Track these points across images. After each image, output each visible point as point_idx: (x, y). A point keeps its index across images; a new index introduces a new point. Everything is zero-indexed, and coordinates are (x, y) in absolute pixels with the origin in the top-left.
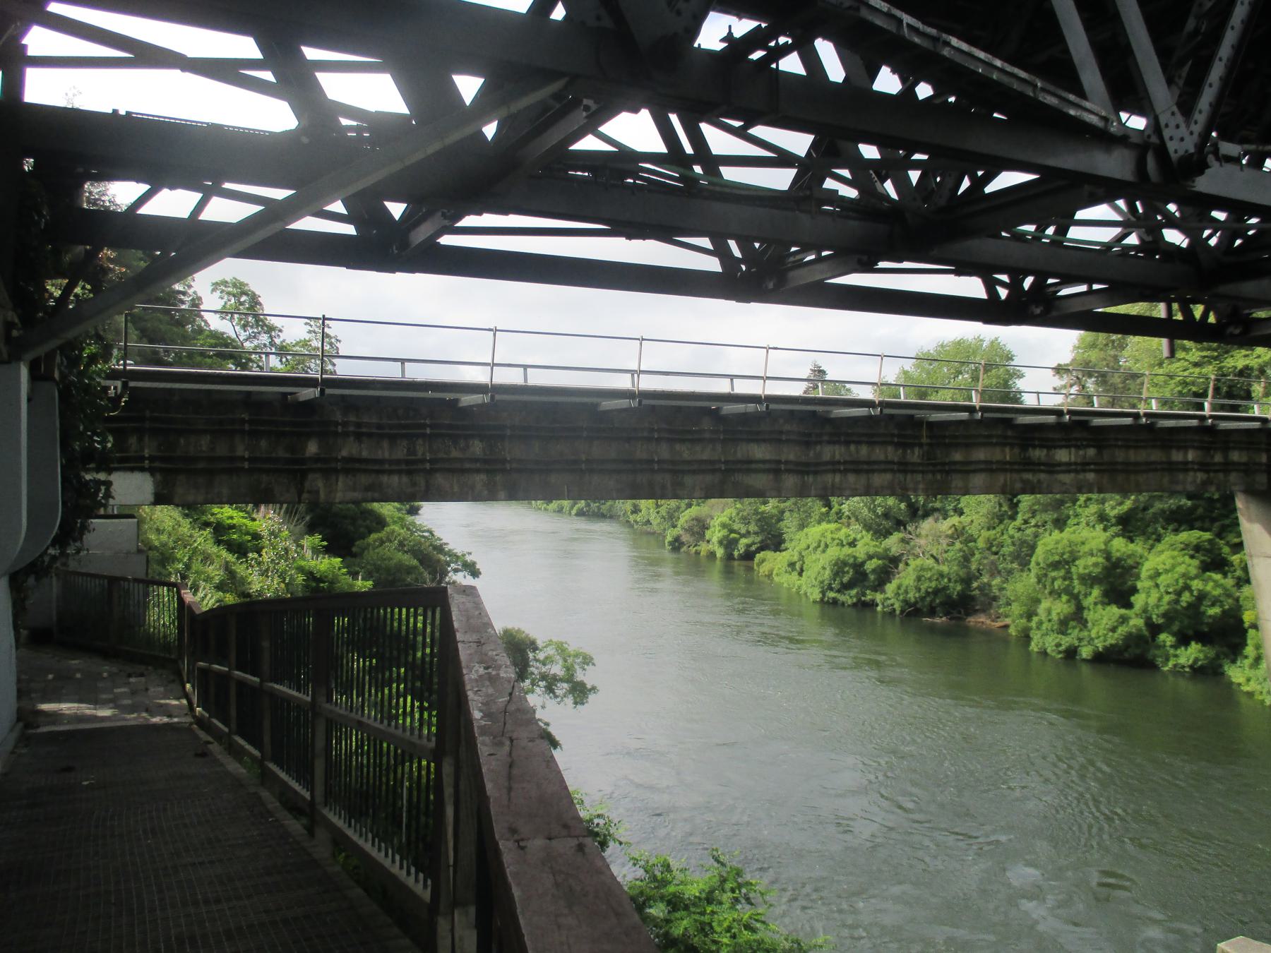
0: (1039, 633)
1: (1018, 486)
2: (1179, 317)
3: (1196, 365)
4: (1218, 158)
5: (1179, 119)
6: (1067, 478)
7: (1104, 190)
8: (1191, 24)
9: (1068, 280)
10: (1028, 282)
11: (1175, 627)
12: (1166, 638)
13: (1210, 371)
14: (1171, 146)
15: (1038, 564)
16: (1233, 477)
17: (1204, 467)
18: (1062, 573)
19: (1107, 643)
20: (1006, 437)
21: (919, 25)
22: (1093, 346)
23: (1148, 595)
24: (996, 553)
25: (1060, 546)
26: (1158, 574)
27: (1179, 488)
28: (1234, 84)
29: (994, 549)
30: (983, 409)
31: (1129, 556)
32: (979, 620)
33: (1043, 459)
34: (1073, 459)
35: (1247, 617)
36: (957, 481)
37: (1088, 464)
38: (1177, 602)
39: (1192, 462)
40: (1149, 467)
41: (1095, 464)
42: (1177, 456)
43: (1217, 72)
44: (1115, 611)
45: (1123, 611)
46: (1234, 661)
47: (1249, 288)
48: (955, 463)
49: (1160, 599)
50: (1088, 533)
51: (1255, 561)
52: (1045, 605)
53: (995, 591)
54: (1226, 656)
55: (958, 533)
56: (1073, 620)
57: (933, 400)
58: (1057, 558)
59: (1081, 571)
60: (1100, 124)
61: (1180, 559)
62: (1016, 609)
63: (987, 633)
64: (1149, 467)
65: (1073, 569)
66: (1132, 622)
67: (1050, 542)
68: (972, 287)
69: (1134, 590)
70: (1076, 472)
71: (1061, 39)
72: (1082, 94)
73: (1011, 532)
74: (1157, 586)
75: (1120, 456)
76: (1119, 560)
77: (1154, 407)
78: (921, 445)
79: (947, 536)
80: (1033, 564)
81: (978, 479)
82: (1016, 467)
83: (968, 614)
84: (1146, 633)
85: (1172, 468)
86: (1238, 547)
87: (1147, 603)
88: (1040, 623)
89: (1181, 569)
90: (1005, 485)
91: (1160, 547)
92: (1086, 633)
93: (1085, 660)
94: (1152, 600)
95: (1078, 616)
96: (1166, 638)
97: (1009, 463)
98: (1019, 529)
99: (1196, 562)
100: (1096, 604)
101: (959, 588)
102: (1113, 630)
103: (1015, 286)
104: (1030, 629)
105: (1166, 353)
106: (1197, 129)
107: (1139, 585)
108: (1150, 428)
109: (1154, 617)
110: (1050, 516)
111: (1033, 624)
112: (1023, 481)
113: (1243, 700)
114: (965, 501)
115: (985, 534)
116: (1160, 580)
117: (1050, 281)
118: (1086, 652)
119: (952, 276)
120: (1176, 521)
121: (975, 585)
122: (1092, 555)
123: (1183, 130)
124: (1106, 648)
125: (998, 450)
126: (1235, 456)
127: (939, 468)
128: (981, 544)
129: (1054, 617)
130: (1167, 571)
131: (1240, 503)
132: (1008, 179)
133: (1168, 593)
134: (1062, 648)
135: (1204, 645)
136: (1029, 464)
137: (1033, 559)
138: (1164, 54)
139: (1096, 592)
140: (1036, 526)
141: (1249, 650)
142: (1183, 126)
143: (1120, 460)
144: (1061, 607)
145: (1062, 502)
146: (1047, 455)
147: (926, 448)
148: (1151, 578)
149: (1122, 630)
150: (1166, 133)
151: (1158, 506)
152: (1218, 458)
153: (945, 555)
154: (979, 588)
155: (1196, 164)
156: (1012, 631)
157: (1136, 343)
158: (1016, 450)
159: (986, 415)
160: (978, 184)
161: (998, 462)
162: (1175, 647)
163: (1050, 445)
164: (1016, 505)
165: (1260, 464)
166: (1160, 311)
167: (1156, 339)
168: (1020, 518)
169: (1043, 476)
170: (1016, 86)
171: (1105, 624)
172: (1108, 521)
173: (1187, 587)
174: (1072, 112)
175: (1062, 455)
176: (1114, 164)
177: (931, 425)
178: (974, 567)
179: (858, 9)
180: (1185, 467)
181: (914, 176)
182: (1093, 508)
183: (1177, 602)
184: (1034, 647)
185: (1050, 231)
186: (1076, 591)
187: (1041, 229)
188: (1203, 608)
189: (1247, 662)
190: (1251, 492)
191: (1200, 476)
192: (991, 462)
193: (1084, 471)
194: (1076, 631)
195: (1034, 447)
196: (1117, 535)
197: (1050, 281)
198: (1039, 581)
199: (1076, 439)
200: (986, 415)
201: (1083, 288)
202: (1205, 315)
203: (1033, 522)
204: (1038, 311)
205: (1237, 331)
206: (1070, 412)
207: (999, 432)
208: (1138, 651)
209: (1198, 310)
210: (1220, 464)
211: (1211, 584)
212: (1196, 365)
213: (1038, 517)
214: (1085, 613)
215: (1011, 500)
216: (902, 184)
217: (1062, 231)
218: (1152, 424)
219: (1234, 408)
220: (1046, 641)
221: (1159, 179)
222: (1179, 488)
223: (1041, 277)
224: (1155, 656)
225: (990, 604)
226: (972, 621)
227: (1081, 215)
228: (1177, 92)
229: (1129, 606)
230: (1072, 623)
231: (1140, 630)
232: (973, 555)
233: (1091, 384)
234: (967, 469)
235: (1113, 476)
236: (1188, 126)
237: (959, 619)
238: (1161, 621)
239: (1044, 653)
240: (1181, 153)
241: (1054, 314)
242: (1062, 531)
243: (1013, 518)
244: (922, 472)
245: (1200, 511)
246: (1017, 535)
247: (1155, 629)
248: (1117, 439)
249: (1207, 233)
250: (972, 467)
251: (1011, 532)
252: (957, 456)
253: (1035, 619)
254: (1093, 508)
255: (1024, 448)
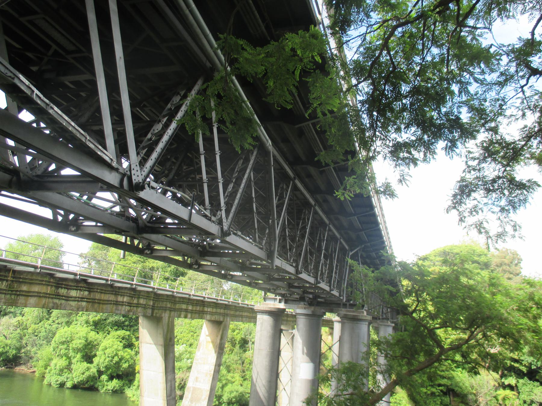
0: (49, 375)
1: (51, 305)
2: (129, 243)
3: (134, 263)
4: (149, 186)
5: (138, 168)
6: (73, 304)
7: (109, 187)
8: (149, 136)
9: (87, 219)
10: (71, 216)
11: (109, 373)
12: (104, 377)
13: (139, 266)
14: (134, 177)
15: (55, 342)
16: (140, 309)
17: (130, 304)
18: (65, 346)
19: (79, 380)
20: (50, 282)
21: (42, 96)
22: (97, 248)
23: (100, 358)
24: (36, 336)
25: (66, 334)
26: (106, 349)
27: (119, 312)
28: (160, 161)
29: (36, 334)
30: (41, 268)
31: (96, 340)
32: (21, 369)
33: (65, 294)
34: (78, 295)
35: (137, 368)
36: (22, 300)
37: (84, 298)
38: (111, 361)
39: (126, 302)
40: (108, 302)
41: (87, 299)
42: (120, 299)
43: (154, 156)
44: (85, 365)
45: (89, 365)
46: (129, 387)
47: (154, 237)
48: (23, 291)
49: (105, 359)
50: (79, 328)
51: (143, 344)
52: (54, 362)
53: (32, 354)
54: (127, 385)
55: (20, 325)
56: (66, 368)
57: (22, 260)
58: (64, 339)
59: (74, 346)
60: (109, 161)
61: (116, 343)
62: (41, 363)
63: (24, 376)
64: (108, 302)
65: (71, 345)
66: (91, 370)
67: (63, 332)
68: (46, 213)
69: (95, 355)
70: (78, 301)
71: (101, 124)
72: (105, 147)
73: (46, 326)
74: (105, 354)
75: (98, 296)
76: (91, 341)
77: (115, 277)
78: (7, 281)
79: (14, 326)
80: (53, 342)
81: (32, 300)
82: (52, 296)
83: (16, 366)
84: (96, 375)
85: (117, 303)
86: (137, 338)
87: (99, 362)
88: (51, 370)
89: (115, 347)
90: (45, 304)
91: (109, 336)
92: (71, 375)
93: (68, 388)
94: (102, 360)
95: (69, 368)
96: (104, 377)
97: (49, 294)
98: (50, 325)
99: (122, 344)
100: (77, 361)
101: (14, 352)
102: (83, 374)
103: (65, 217)
104: (45, 373)
105: (122, 256)
106: (144, 174)
107: (97, 353)
108: (112, 286)
109: (101, 368)
110: (65, 320)
111: (47, 371)
112: (54, 303)
113: (131, 403)
114: (26, 310)
115: (33, 326)
116: (106, 351)
117: (81, 218)
118: (69, 384)
119: (37, 206)
120: (117, 325)
121: (23, 351)
122: (80, 339)
123: (139, 173)
124: (78, 382)
125: (45, 287)
126: (142, 301)
127: (14, 292)
128: (30, 331)
129: (58, 367)
130: (110, 347)
131: (141, 320)
132: (67, 172)
133: (109, 357)
134: (59, 382)
135: (119, 380)
136: (58, 295)
137: (54, 339)
138: (138, 143)
139: (79, 356)
140: (58, 324)
141: (136, 383)
142: (139, 171)
143: (97, 298)
144: (63, 362)
145: (71, 314)
146: (67, 292)
147: (9, 282)
148: (103, 350)
149: (87, 374)
150: (133, 172)
151: (111, 319)
152: (135, 301)
153: (10, 335)
154: (24, 353)
155: (140, 187)
156: (37, 374)
157: (113, 250)
158: (53, 288)
159: (42, 271)
160: (58, 169)
161: (44, 293)
162: (107, 381)
163: (68, 288)
164: (51, 313)
165: (150, 305)
166: (122, 239)
167: (119, 250)
168: (51, 319)
169: (63, 302)
170: (78, 135)
171: (80, 371)
172: (89, 323)
173: (117, 355)
174: (99, 153)
175: (73, 293)
176: (112, 178)
177: (14, 272)
178: (24, 342)
179: (13, 79)
180: (122, 304)
181: (29, 158)
182: (84, 318)
183: (111, 361)
184: (45, 382)
185: (85, 197)
186: (70, 355)
187: (81, 196)
188: (121, 364)
189: (134, 388)
190: (145, 316)
191: (128, 308)
192: (40, 293)
193: (82, 301)
194: (67, 374)
195: (62, 288)
196: (92, 330)
197: (81, 218)
198: (54, 350)
199: (81, 287)
200: (42, 271)
201: (94, 224)
202: (139, 244)
203: (57, 321)
204: (73, 229)
205: (148, 252)
206: (80, 275)
207: (47, 279)
208: (92, 383)
209: (136, 242)
210: (135, 304)
211: (126, 353)
212: (134, 263)
213: (59, 320)
214: (72, 365)
215: (49, 311)
216: (22, 160)
217: (90, 199)
218: (113, 284)
219: (146, 282)
220: (52, 379)
221: (129, 189)
222: (119, 312)
223: (77, 215)
224: (98, 385)
225: (28, 361)
226: (17, 369)
227: (99, 194)
228: (140, 158)
229: (91, 362)
230: (66, 370)
231: (94, 374)
232: (25, 336)
233: (93, 263)
234: (28, 295)
235: (94, 304)
236: (141, 172)
237: (12, 368)
238: (103, 369)
239: (50, 385)
240: (137, 181)
241: (80, 232)
242: (69, 327)
243: (48, 319)
244: (5, 294)
245: (127, 323)
246: (48, 327)
247: (100, 373)
248: (98, 289)
249: (143, 213)
250: (31, 294)
251: (46, 326)
252: (25, 288)
253: (49, 368)
254: (84, 318)
255: (57, 288)
